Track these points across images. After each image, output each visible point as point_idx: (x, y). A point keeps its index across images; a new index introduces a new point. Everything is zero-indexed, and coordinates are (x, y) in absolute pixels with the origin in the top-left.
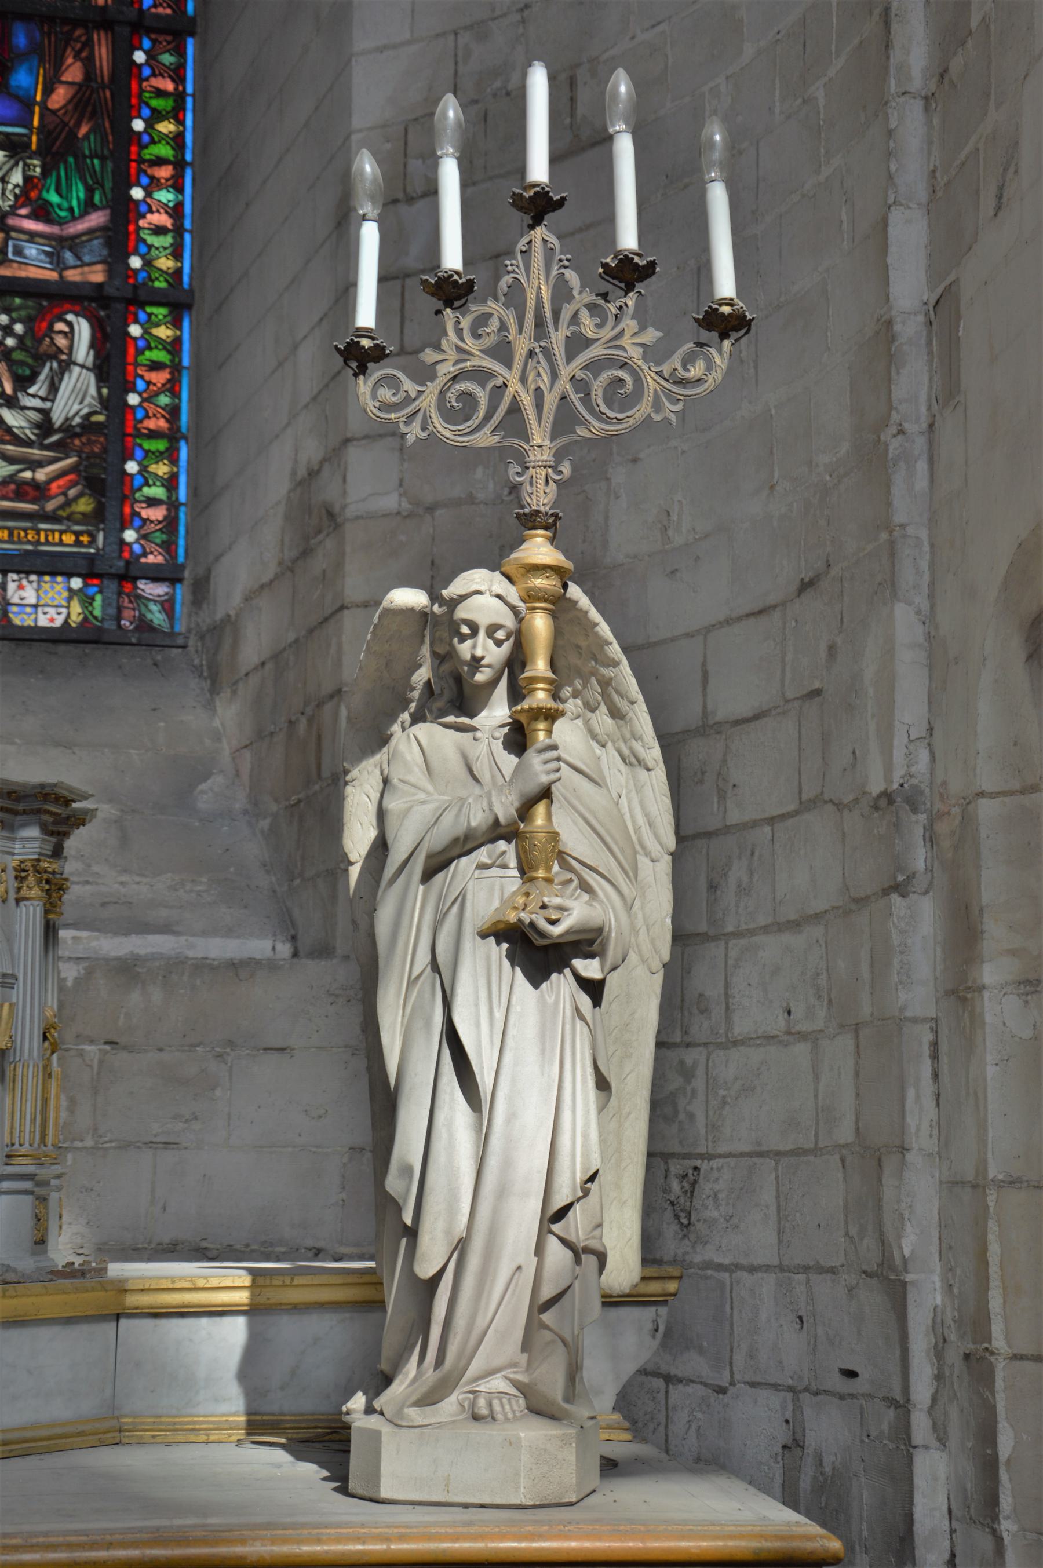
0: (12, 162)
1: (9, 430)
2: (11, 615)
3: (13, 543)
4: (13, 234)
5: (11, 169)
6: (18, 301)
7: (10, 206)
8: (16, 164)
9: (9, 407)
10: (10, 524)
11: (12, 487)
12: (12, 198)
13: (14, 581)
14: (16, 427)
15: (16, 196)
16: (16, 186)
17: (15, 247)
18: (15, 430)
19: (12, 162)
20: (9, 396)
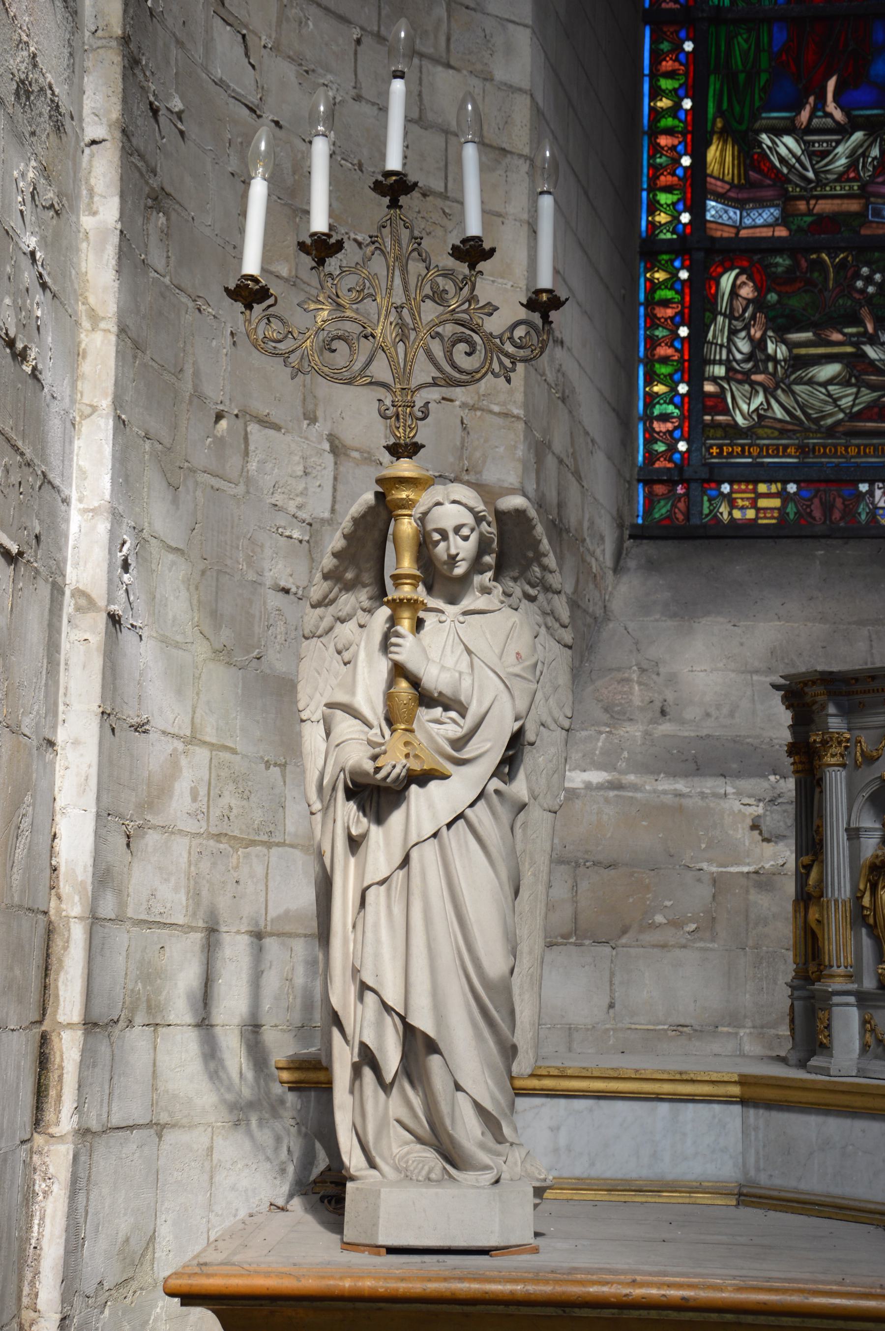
0: (871, 139)
1: (872, 362)
2: (879, 517)
3: (878, 457)
4: (872, 199)
5: (870, 145)
6: (877, 254)
7: (869, 176)
8: (875, 141)
9: (872, 344)
10: (875, 441)
11: (876, 410)
12: (871, 169)
13: (879, 488)
14: (878, 360)
15: (874, 167)
16: (875, 158)
17: (874, 210)
18: (877, 363)
19: (871, 139)
20: (871, 335)
